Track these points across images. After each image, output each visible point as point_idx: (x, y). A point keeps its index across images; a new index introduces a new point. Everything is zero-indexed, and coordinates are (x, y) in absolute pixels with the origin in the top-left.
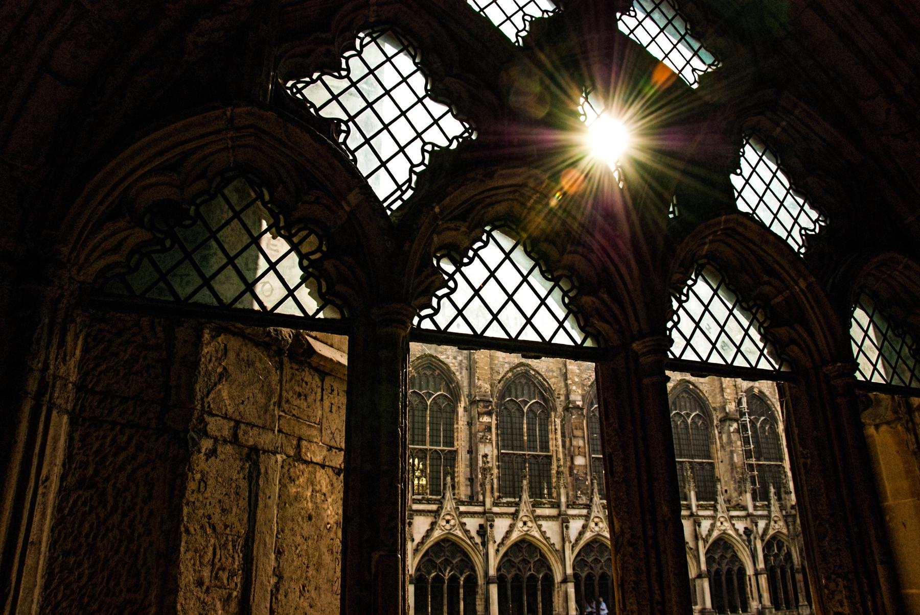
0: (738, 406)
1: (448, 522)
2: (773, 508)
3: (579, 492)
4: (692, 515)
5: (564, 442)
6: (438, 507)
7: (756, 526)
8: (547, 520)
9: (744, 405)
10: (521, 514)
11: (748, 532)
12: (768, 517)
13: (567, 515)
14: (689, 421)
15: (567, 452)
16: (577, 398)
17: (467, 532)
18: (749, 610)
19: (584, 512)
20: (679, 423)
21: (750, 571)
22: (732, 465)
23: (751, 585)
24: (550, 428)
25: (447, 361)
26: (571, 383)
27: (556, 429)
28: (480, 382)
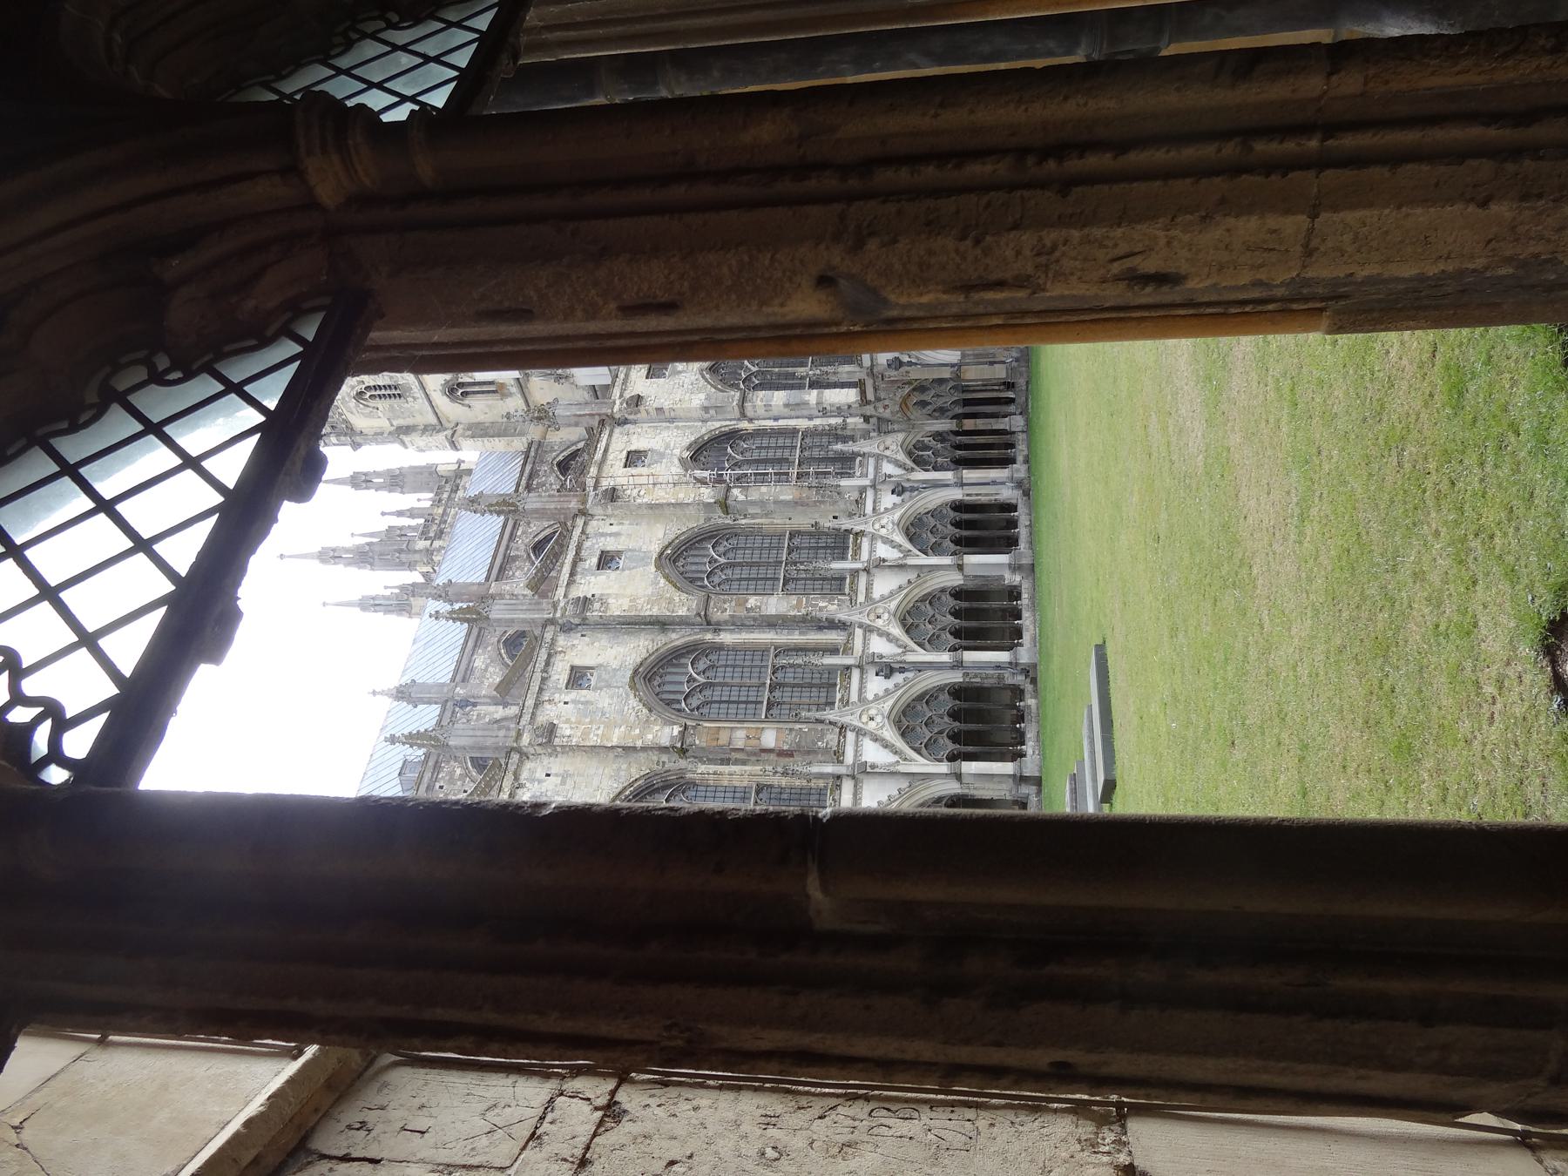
0: (706, 483)
2: (866, 450)
4: (867, 570)
5: (737, 762)
7: (890, 476)
8: (860, 799)
9: (706, 474)
11: (899, 490)
12: (879, 458)
13: (854, 764)
14: (722, 560)
15: (754, 758)
16: (666, 733)
18: (1014, 501)
19: (851, 736)
20: (724, 577)
21: (957, 494)
22: (796, 503)
23: (977, 495)
24: (711, 782)
26: (641, 741)
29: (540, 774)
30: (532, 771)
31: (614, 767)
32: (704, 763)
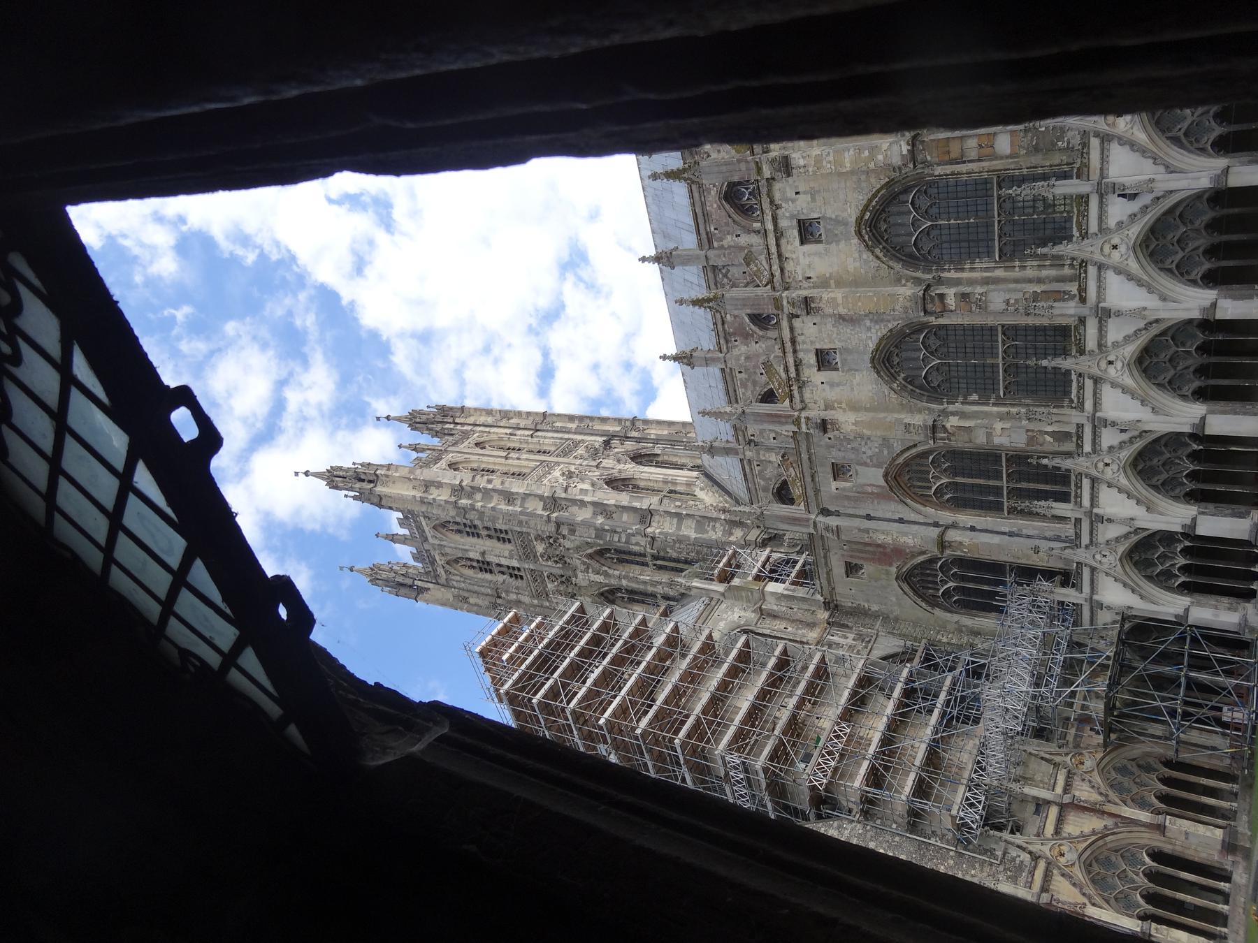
1: (1107, 465)
3: (1060, 143)
6: (1086, 477)
10: (1095, 371)
17: (1122, 445)
25: (875, 340)
27: (953, 174)
28: (897, 307)
29: (792, 195)
30: (783, 192)
31: (854, 178)
32: (939, 164)
